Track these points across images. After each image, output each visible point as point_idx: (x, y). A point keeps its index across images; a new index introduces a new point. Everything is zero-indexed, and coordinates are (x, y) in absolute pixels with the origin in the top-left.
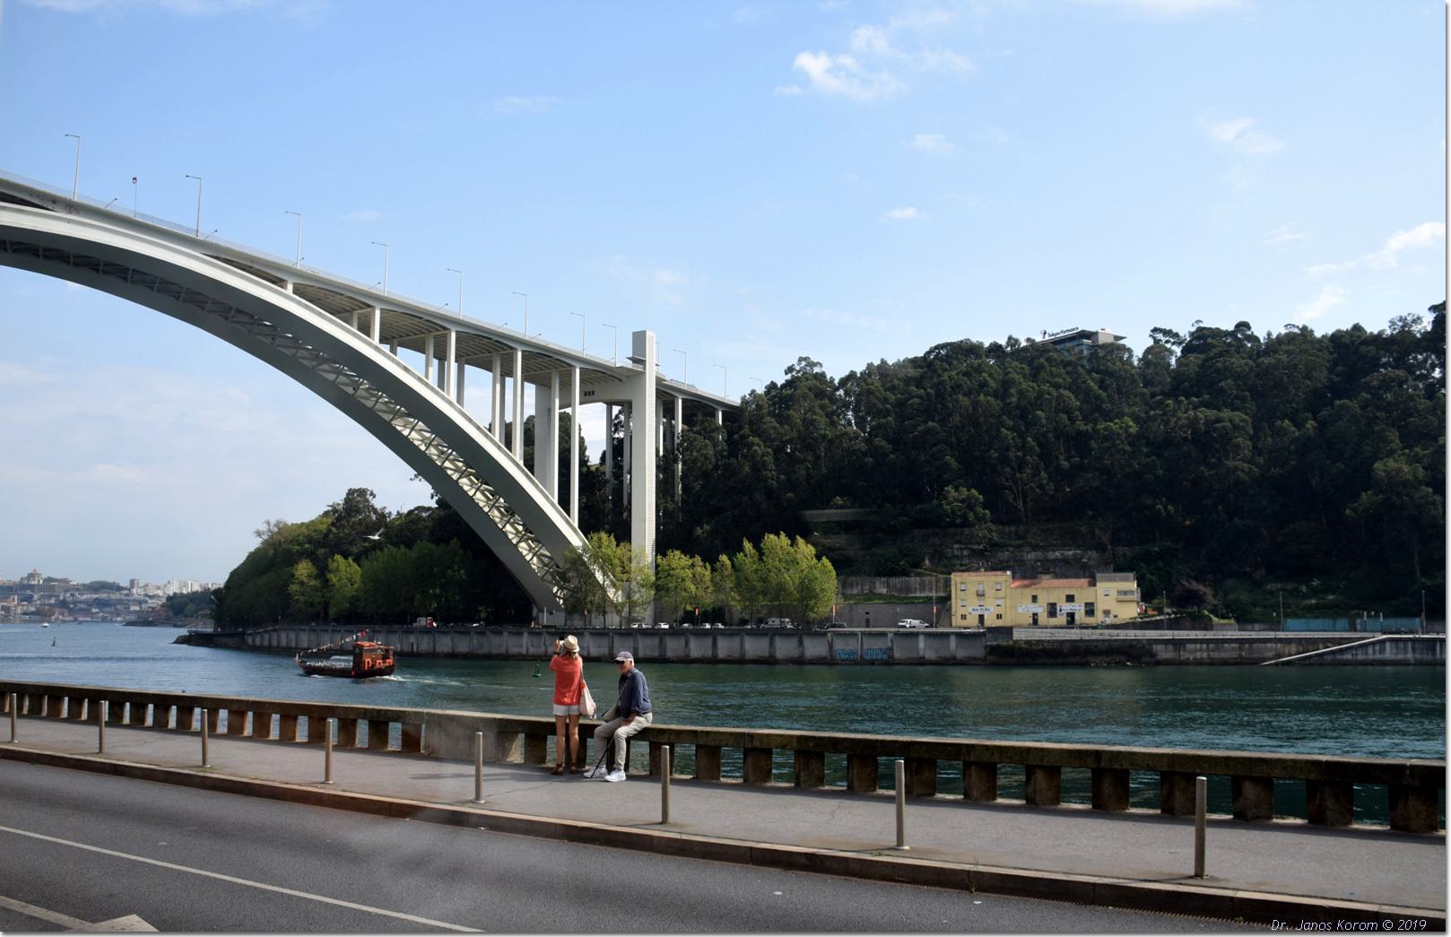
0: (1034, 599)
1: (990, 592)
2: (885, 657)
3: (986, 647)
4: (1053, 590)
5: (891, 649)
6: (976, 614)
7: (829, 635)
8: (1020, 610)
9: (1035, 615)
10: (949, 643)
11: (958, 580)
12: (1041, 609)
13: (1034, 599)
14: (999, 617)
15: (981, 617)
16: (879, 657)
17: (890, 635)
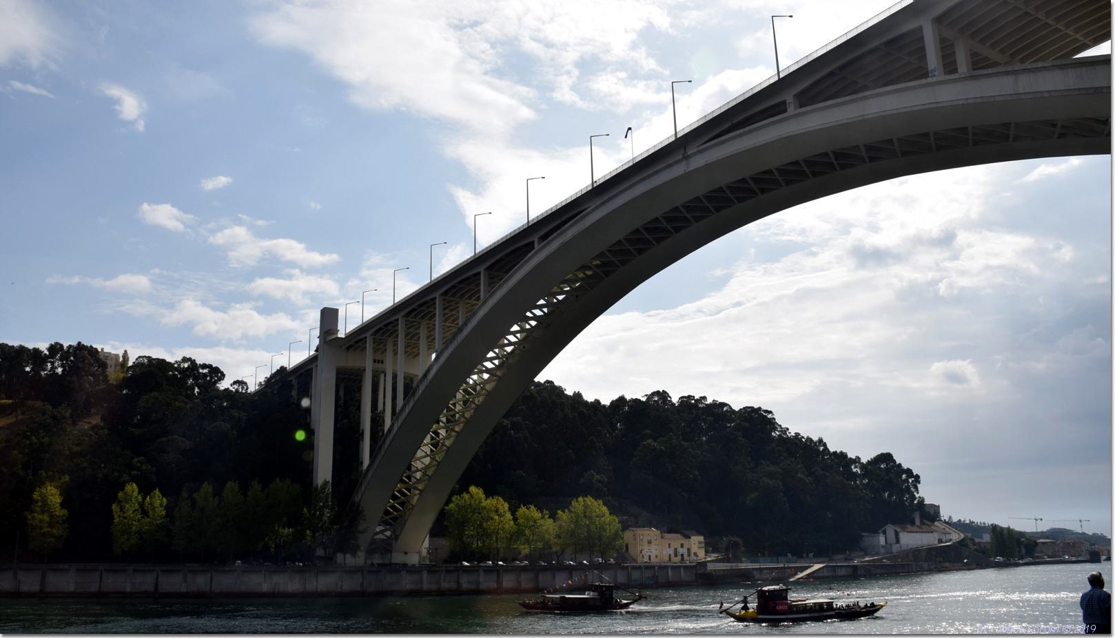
0: (669, 544)
1: (653, 540)
2: (652, 582)
3: (696, 574)
4: (676, 540)
5: (657, 577)
6: (648, 554)
7: (630, 568)
8: (664, 552)
9: (670, 555)
10: (680, 571)
11: (640, 532)
12: (672, 552)
13: (669, 544)
14: (657, 556)
15: (650, 556)
16: (647, 582)
17: (656, 568)
